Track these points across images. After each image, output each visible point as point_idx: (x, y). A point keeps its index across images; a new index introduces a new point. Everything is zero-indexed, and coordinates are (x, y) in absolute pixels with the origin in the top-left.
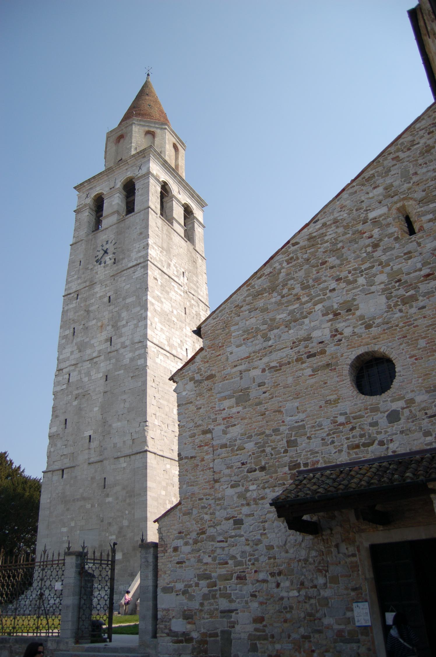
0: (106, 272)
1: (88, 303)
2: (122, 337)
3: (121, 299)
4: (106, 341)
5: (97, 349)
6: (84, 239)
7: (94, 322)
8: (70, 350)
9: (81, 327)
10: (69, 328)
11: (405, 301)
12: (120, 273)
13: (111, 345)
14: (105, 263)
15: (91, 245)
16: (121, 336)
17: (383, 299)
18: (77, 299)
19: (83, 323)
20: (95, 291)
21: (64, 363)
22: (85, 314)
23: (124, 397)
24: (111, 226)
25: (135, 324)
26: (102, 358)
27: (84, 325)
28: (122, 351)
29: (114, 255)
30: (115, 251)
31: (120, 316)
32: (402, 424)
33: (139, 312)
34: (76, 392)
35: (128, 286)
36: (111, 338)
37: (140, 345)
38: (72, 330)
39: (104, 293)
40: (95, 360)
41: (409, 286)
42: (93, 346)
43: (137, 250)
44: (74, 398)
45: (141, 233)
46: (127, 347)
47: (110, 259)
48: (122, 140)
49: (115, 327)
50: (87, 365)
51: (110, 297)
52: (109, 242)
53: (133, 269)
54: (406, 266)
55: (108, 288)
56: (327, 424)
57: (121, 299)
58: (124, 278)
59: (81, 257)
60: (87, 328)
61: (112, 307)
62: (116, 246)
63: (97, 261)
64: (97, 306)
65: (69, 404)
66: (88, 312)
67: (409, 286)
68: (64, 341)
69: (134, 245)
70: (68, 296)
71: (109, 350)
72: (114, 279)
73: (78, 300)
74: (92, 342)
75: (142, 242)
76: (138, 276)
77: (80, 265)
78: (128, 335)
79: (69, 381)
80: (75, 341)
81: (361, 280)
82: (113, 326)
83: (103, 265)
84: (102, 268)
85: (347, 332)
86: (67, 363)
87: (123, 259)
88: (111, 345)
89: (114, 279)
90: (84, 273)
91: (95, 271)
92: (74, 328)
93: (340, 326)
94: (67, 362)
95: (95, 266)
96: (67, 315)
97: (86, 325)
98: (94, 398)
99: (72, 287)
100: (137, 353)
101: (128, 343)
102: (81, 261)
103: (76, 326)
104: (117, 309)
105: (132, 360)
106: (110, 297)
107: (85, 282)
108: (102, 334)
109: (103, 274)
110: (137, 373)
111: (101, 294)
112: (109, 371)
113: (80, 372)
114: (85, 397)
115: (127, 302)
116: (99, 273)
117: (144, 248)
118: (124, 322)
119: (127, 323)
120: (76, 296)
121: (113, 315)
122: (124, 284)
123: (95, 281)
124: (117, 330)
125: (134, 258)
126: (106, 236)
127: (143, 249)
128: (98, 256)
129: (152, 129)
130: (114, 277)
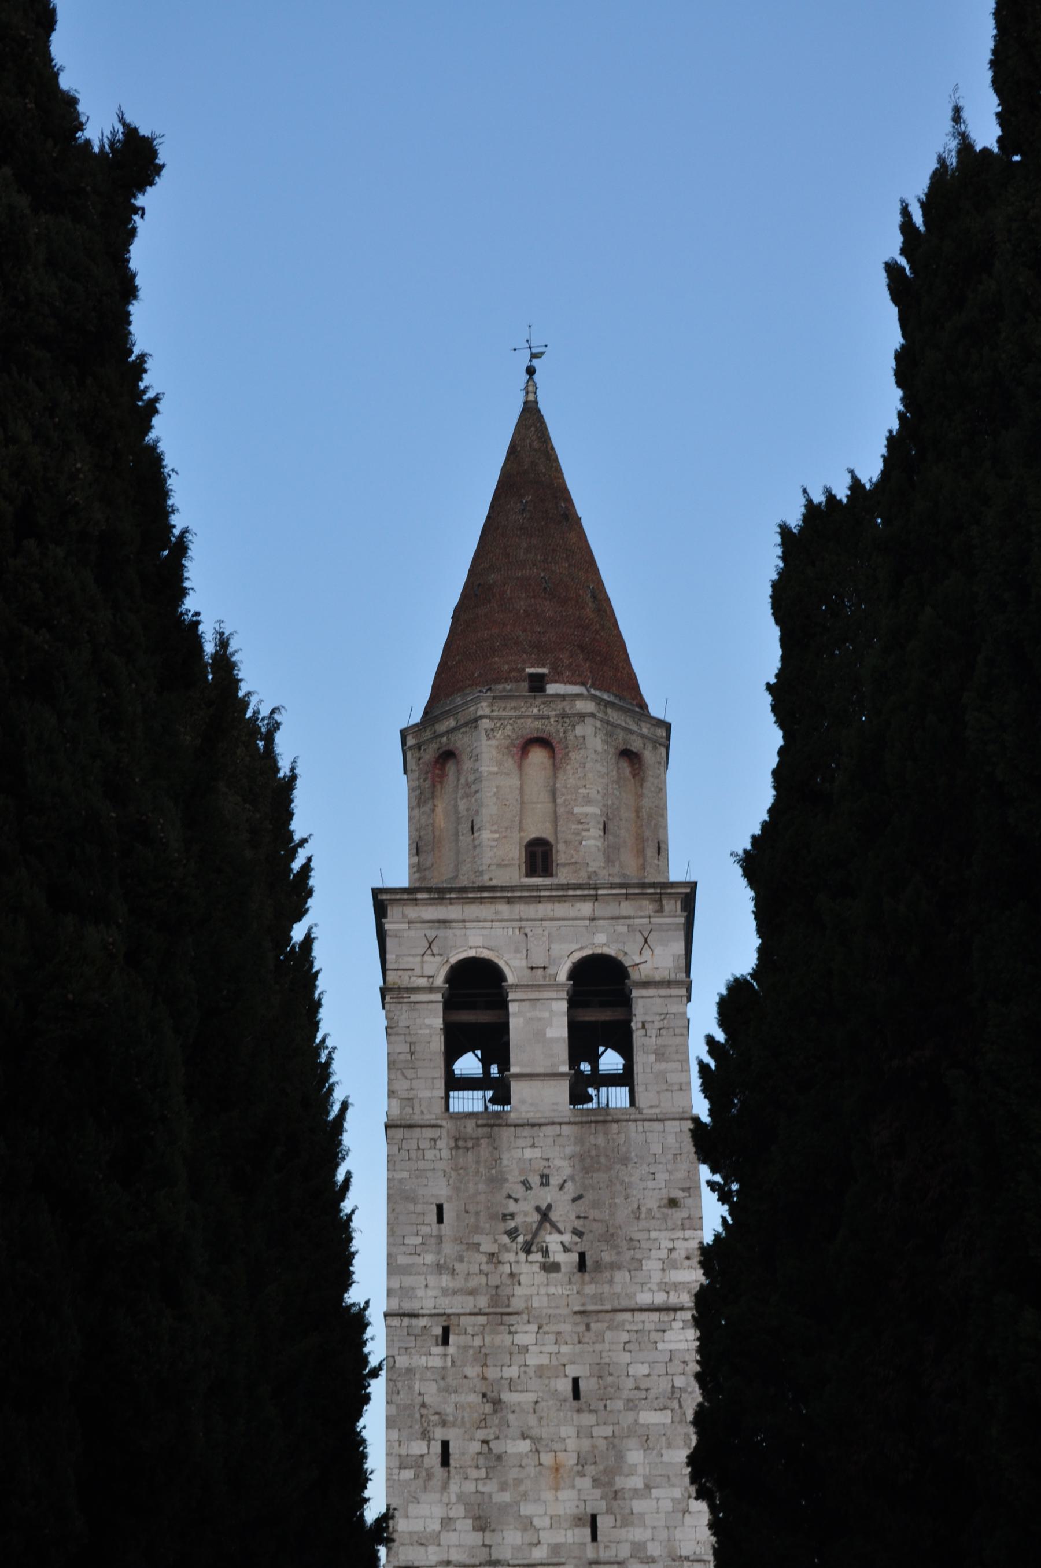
0: (552, 1290)
1: (492, 1373)
2: (632, 1524)
3: (619, 1405)
4: (577, 1521)
6: (439, 1122)
7: (525, 1446)
8: (438, 1512)
9: (475, 1447)
10: (425, 1435)
12: (607, 1312)
13: (594, 1538)
14: (546, 1252)
15: (478, 1162)
16: (627, 1520)
18: (445, 1341)
19: (481, 1434)
20: (521, 1339)
21: (422, 1549)
22: (488, 1408)
24: (553, 1123)
25: (673, 1500)
27: (485, 1442)
29: (577, 1239)
30: (579, 1224)
31: (620, 1457)
35: (644, 1370)
36: (594, 1518)
38: (437, 1448)
39: (554, 1362)
42: (527, 1524)
43: (663, 1254)
45: (673, 1203)
47: (566, 1249)
48: (538, 756)
49: (605, 1482)
51: (576, 1381)
52: (555, 1181)
53: (655, 1316)
55: (564, 1349)
57: (619, 1405)
58: (625, 1337)
59: (440, 1189)
60: (499, 1458)
61: (588, 1419)
62: (581, 1207)
63: (512, 1234)
64: (531, 1397)
66: (497, 1403)
68: (408, 1474)
69: (653, 1235)
70: (406, 1321)
71: (590, 1553)
72: (588, 1327)
73: (451, 1350)
75: (679, 1234)
76: (673, 1346)
77: (440, 1220)
78: (654, 1528)
80: (454, 1488)
82: (596, 1482)
83: (537, 1257)
84: (536, 1268)
87: (615, 1266)
88: (594, 1538)
89: (588, 1327)
90: (461, 1259)
91: (507, 1269)
92: (445, 1445)
94: (432, 1549)
95: (505, 1248)
96: (411, 1388)
97: (496, 1447)
99: (420, 1293)
101: (654, 1550)
102: (440, 1208)
103: (453, 1435)
104: (608, 1431)
106: (576, 1381)
107: (473, 1292)
108: (563, 1495)
109: (543, 1291)
111: (544, 1360)
115: (641, 1421)
116: (523, 1279)
117: (688, 1258)
118: (636, 1482)
119: (648, 1487)
120: (438, 1331)
121: (594, 1447)
122: (626, 1357)
123: (517, 1304)
124: (615, 1498)
125: (656, 1277)
126: (537, 1153)
127: (687, 1263)
128: (512, 1216)
129: (636, 745)
130: (585, 1320)
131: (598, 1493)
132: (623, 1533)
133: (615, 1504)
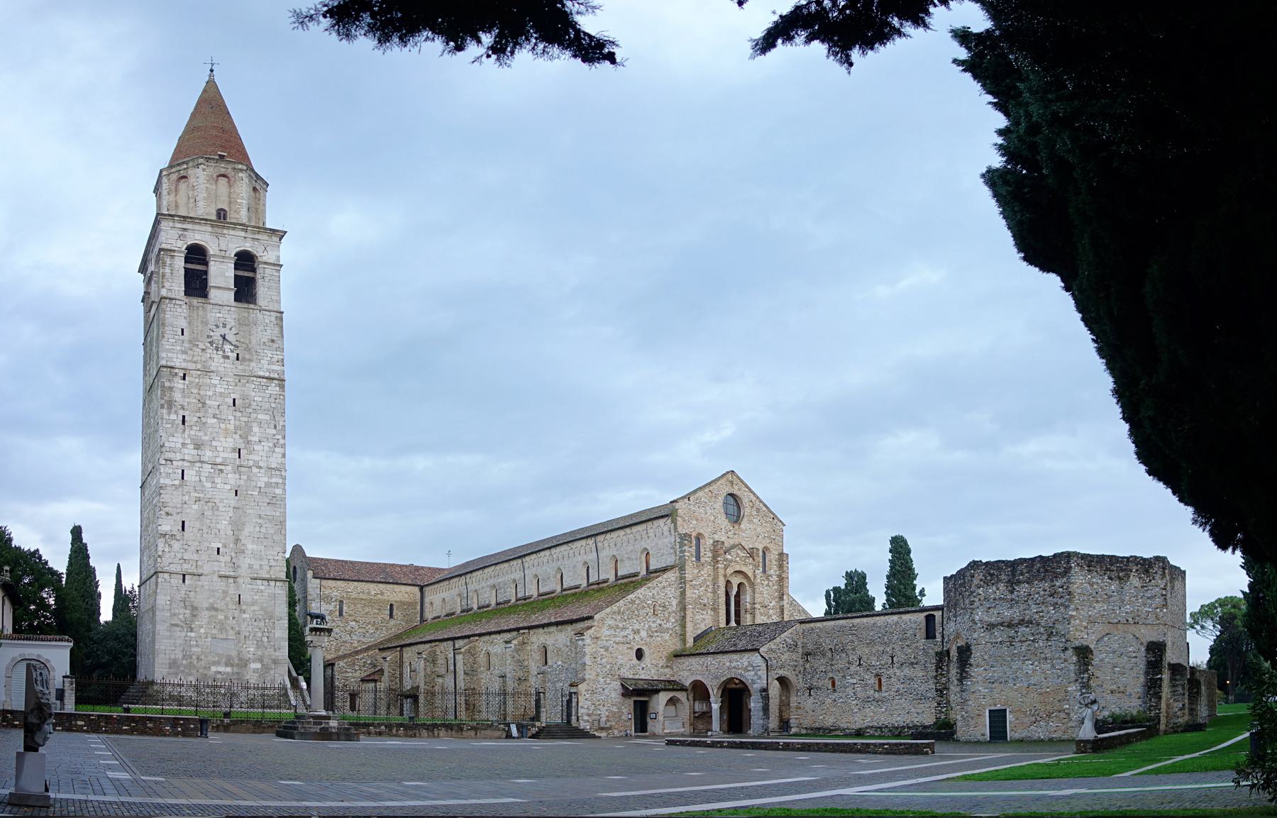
4: (234, 450)
5: (222, 455)
11: (651, 636)
13: (239, 457)
17: (646, 633)
23: (261, 521)
26: (229, 468)
28: (255, 470)
31: (250, 429)
32: (644, 671)
33: (274, 435)
34: (197, 495)
36: (240, 450)
37: (278, 472)
40: (219, 467)
41: (652, 632)
44: (194, 499)
46: (260, 468)
49: (245, 437)
50: (207, 468)
54: (654, 625)
56: (628, 666)
65: (185, 506)
67: (652, 632)
74: (214, 443)
79: (183, 478)
81: (642, 624)
82: (240, 436)
85: (637, 639)
86: (179, 456)
88: (239, 457)
93: (636, 637)
94: (178, 454)
98: (220, 509)
100: (274, 480)
101: (261, 464)
105: (268, 485)
110: (274, 501)
112: (239, 486)
113: (199, 474)
114: (209, 504)
124: (248, 443)
131: (241, 441)
132: (251, 457)
133: (248, 446)
